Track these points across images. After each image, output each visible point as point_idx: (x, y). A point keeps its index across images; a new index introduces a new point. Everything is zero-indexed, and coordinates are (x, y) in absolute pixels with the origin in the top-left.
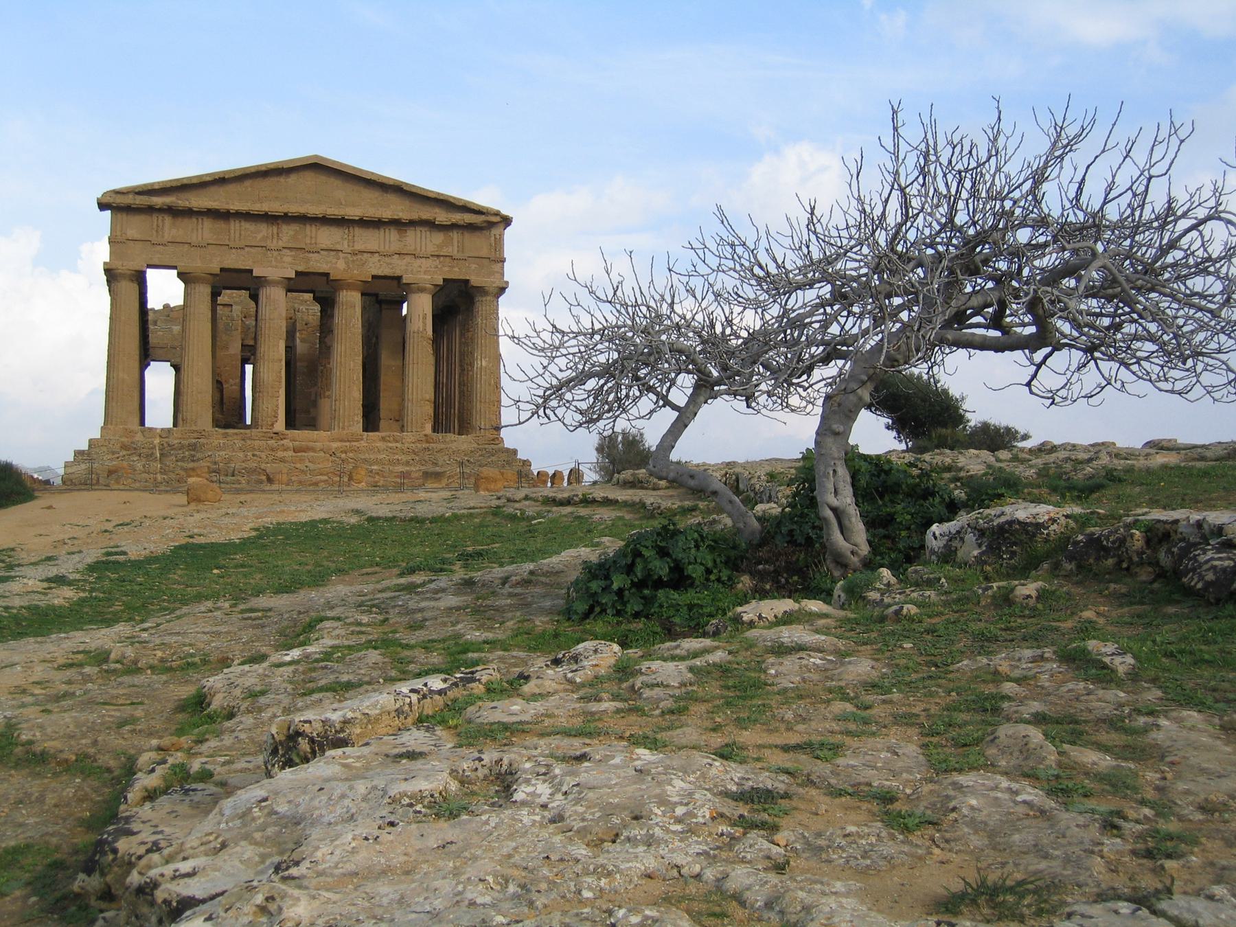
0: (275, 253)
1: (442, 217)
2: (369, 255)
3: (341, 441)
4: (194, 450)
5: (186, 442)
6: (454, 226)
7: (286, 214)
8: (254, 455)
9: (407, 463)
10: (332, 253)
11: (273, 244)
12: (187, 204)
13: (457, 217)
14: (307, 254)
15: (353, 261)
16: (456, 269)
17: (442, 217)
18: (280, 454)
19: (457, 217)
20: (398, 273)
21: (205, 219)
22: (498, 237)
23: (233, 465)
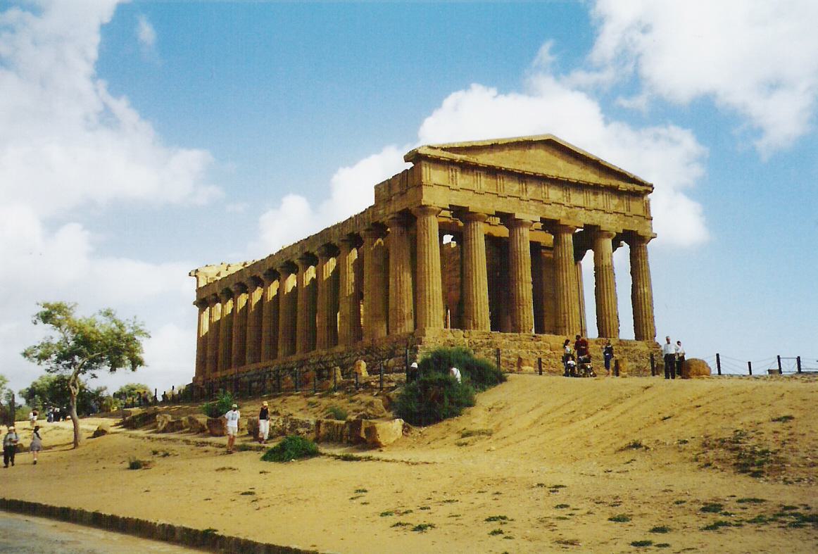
0: (526, 202)
1: (623, 186)
2: (579, 209)
5: (485, 341)
7: (535, 174)
10: (558, 206)
11: (524, 197)
12: (474, 160)
13: (630, 186)
14: (544, 205)
15: (570, 213)
16: (627, 223)
17: (623, 186)
19: (630, 186)
20: (596, 223)
21: (482, 172)
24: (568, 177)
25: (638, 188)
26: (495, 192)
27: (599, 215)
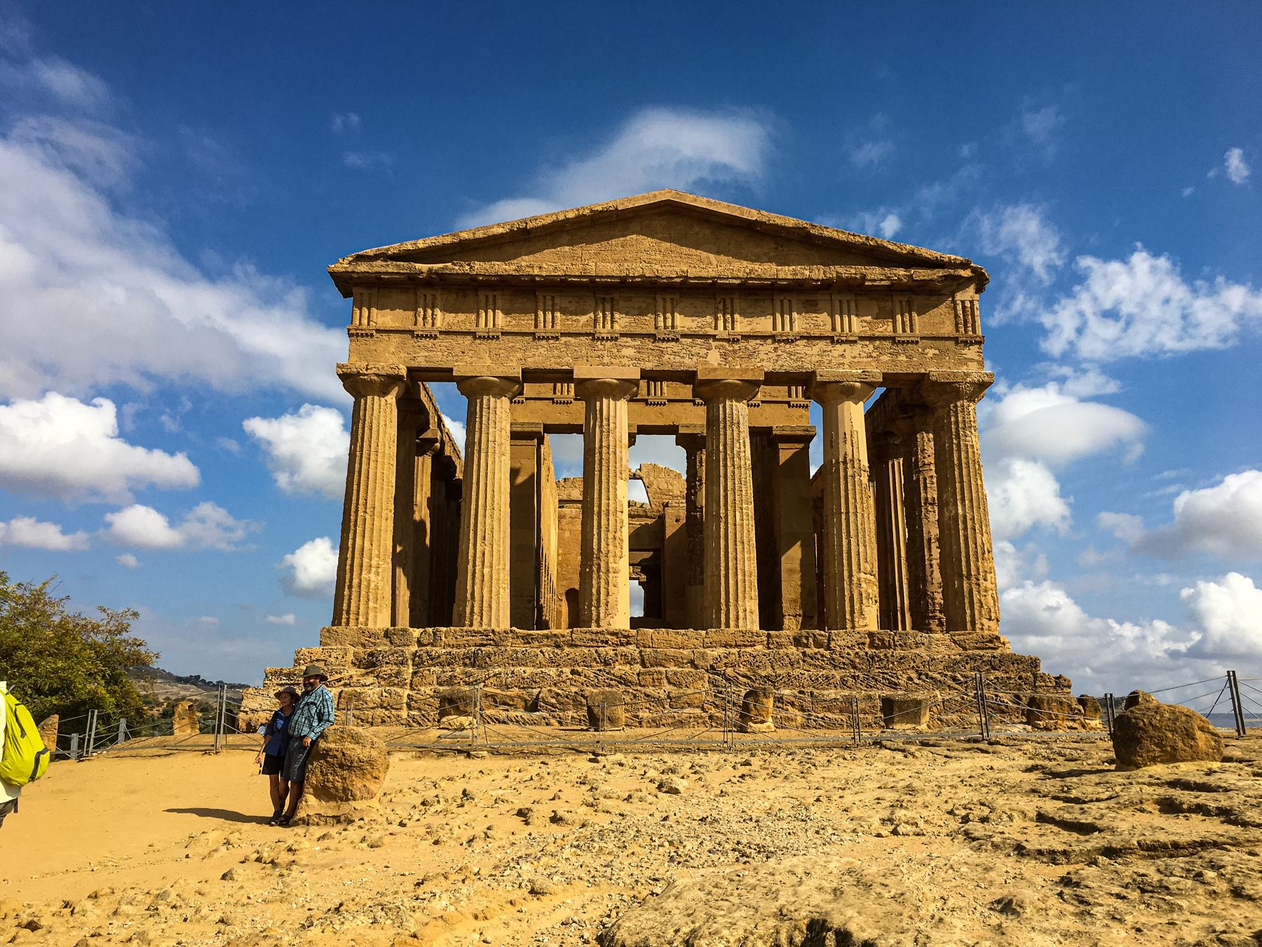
1: (875, 274)
2: (758, 341)
3: (725, 647)
4: (473, 665)
6: (894, 289)
8: (573, 672)
9: (843, 682)
10: (699, 341)
14: (660, 344)
15: (734, 351)
16: (903, 358)
18: (620, 669)
20: (808, 367)
21: (498, 294)
22: (968, 305)
23: (536, 691)
24: (714, 274)
25: (921, 274)
26: (532, 329)
27: (816, 349)
